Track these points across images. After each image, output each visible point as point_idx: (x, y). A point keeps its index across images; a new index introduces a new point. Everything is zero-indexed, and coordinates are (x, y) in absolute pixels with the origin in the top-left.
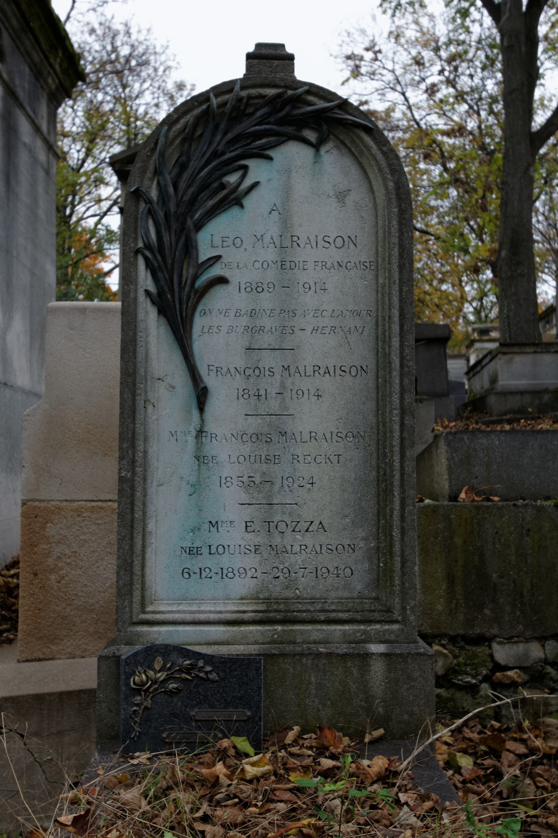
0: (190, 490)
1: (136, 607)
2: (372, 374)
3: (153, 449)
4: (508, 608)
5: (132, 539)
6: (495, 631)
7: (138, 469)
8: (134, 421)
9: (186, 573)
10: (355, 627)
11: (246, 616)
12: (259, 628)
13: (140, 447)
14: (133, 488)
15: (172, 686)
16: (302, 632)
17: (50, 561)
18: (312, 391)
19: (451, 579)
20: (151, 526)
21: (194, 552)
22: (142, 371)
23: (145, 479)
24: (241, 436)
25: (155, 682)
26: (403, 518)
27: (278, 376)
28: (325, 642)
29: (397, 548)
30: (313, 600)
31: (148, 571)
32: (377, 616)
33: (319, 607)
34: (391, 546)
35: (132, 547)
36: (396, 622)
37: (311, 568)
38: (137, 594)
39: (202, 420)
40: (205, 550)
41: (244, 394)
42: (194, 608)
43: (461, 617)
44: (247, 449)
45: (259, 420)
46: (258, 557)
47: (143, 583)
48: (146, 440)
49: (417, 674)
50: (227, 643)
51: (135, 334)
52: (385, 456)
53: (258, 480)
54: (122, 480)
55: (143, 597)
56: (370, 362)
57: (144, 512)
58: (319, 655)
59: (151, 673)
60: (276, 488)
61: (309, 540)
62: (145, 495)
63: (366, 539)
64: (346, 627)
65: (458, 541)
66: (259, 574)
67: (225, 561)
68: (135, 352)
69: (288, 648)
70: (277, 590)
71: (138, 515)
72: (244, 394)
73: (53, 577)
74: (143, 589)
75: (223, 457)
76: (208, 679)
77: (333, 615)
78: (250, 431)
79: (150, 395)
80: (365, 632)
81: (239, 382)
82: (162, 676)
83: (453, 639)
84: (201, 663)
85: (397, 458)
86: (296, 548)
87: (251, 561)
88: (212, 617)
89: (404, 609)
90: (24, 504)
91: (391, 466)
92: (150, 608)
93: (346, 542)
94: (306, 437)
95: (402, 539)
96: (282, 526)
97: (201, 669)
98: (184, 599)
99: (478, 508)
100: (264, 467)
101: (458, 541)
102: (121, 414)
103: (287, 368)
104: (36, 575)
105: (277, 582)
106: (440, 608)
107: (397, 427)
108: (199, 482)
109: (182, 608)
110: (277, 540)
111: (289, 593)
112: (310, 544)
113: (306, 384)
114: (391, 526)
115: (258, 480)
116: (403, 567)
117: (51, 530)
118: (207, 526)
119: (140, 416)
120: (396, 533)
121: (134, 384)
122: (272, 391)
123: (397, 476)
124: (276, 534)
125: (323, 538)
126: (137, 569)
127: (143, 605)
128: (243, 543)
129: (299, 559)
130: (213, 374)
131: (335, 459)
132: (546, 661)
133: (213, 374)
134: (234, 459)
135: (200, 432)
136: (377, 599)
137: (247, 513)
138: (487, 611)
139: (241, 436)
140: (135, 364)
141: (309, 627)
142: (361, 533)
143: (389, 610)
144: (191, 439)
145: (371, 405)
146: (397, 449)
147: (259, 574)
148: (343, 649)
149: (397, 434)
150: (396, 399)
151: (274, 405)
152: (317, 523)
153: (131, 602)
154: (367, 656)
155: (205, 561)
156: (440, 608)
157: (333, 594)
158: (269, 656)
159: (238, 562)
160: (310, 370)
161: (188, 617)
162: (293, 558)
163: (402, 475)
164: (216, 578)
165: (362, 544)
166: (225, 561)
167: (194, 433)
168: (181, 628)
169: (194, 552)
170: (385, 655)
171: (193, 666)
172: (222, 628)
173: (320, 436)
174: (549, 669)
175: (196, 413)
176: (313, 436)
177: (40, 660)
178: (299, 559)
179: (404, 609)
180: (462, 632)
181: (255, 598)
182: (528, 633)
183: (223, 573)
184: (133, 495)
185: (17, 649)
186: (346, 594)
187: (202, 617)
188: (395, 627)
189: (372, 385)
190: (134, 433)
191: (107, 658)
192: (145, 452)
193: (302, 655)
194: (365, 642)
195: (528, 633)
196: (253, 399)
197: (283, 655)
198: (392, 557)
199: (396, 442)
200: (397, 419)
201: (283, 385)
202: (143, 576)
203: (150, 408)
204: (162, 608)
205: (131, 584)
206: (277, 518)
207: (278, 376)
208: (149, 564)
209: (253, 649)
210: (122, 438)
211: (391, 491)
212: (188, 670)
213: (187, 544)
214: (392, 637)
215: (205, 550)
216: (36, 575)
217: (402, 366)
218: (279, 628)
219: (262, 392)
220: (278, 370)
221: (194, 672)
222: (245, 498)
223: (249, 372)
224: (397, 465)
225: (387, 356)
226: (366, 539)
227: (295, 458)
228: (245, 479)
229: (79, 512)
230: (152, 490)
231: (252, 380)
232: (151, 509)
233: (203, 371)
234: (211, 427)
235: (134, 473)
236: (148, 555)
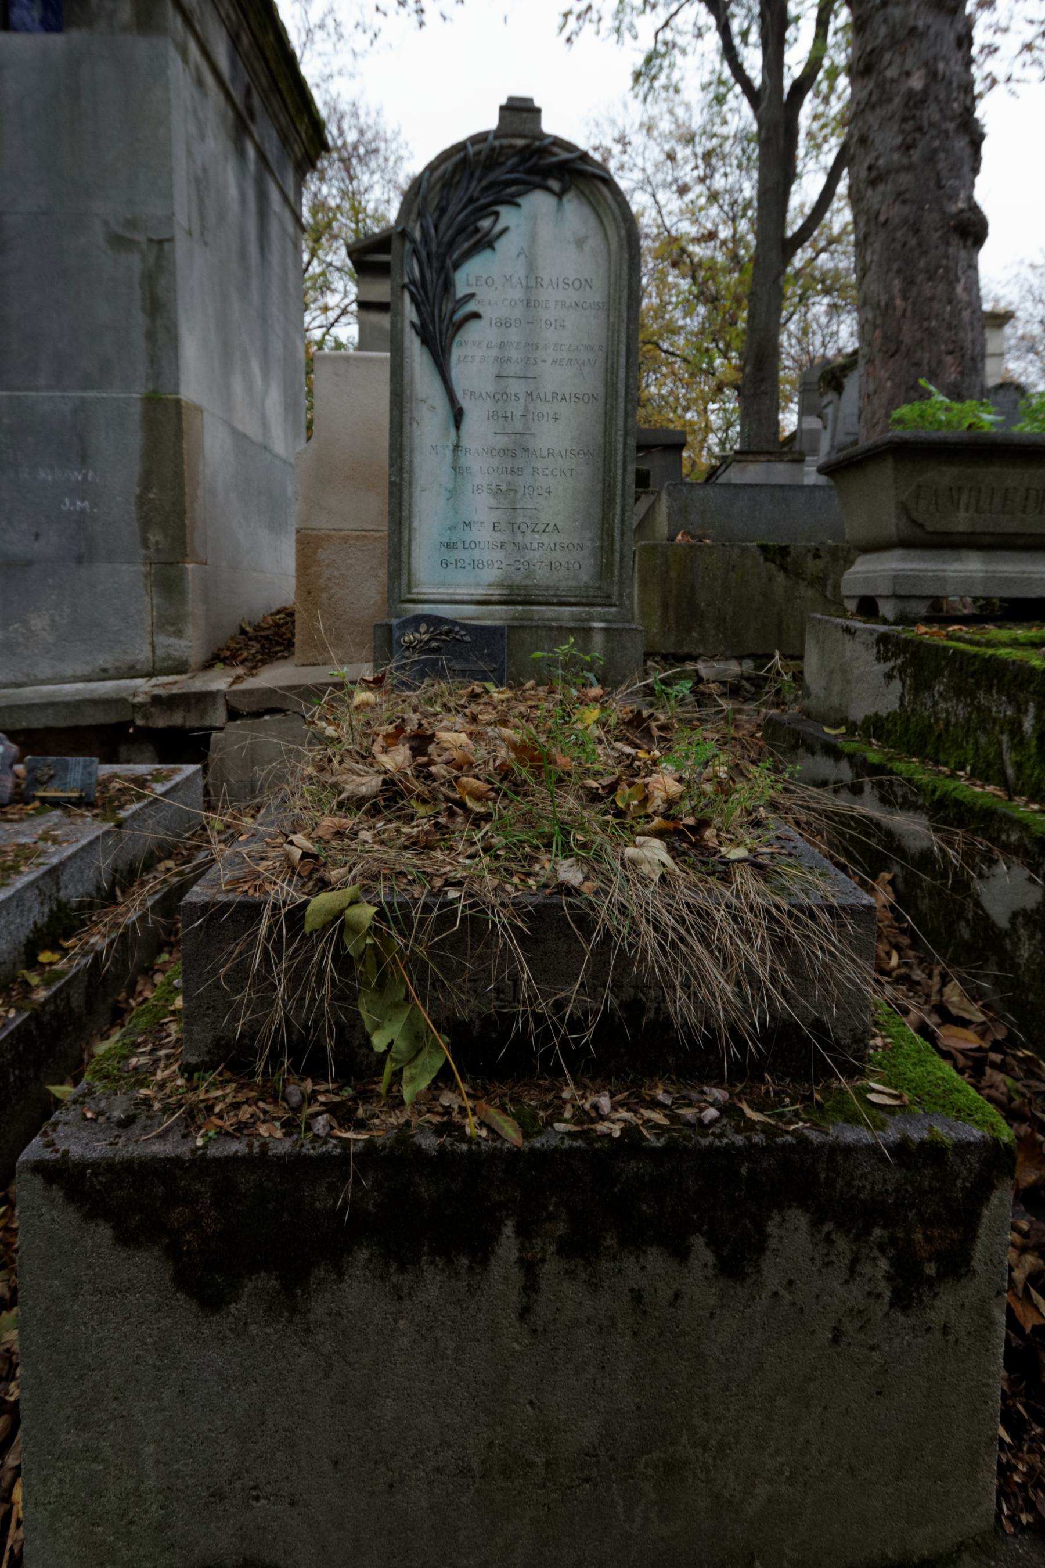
0: (448, 495)
1: (404, 588)
2: (601, 401)
3: (418, 460)
4: (713, 632)
5: (400, 533)
6: (701, 650)
7: (405, 476)
8: (401, 433)
9: (444, 563)
10: (581, 609)
11: (493, 598)
12: (504, 607)
13: (407, 458)
14: (401, 491)
15: (434, 644)
16: (538, 612)
17: (322, 582)
18: (551, 414)
19: (665, 607)
20: (415, 524)
21: (450, 546)
22: (408, 392)
23: (410, 484)
24: (491, 451)
25: (420, 641)
26: (623, 522)
27: (522, 401)
28: (556, 620)
29: (617, 545)
30: (547, 588)
31: (413, 560)
32: (599, 601)
33: (552, 593)
34: (612, 544)
35: (400, 540)
36: (614, 605)
37: (546, 562)
38: (405, 578)
39: (458, 437)
40: (460, 545)
41: (494, 415)
42: (451, 591)
43: (672, 638)
44: (495, 462)
45: (506, 438)
46: (503, 552)
47: (409, 570)
48: (411, 451)
49: (629, 645)
50: (478, 619)
51: (402, 359)
52: (610, 470)
53: (504, 488)
54: (392, 484)
55: (409, 581)
56: (600, 391)
57: (410, 512)
58: (551, 628)
59: (417, 635)
60: (519, 495)
61: (545, 539)
62: (411, 498)
63: (592, 539)
64: (574, 609)
65: (673, 574)
66: (504, 566)
67: (476, 554)
68: (402, 376)
69: (526, 623)
70: (518, 578)
71: (405, 513)
72: (494, 415)
73: (324, 595)
74: (409, 574)
75: (475, 468)
76: (462, 641)
77: (564, 599)
78: (498, 447)
79: (415, 414)
80: (589, 613)
81: (489, 405)
82: (426, 637)
83: (665, 657)
84: (457, 629)
85: (620, 472)
86: (535, 545)
87: (498, 555)
88: (466, 598)
89: (621, 595)
90: (298, 532)
91: (615, 478)
92: (415, 590)
93: (576, 541)
94: (545, 453)
95: (622, 540)
96: (523, 527)
97: (457, 633)
98: (443, 584)
99: (692, 547)
100: (510, 477)
101: (673, 574)
102: (391, 428)
103: (530, 394)
104: (309, 593)
105: (518, 573)
106: (655, 630)
107: (620, 446)
108: (455, 489)
109: (441, 590)
110: (519, 538)
111: (528, 582)
112: (546, 542)
113: (545, 408)
114: (613, 529)
115: (504, 488)
116: (621, 561)
117: (322, 555)
118: (461, 525)
119: (406, 431)
120: (617, 534)
121: (401, 403)
122: (518, 414)
123: (619, 486)
124: (519, 533)
125: (557, 538)
126: (404, 558)
127: (409, 587)
128: (491, 540)
129: (537, 555)
130: (467, 397)
131: (568, 473)
132: (742, 677)
133: (467, 397)
134: (484, 470)
135: (457, 447)
136: (599, 588)
137: (494, 516)
138: (695, 634)
139: (491, 451)
140: (402, 386)
141: (544, 608)
142: (589, 534)
143: (609, 597)
144: (449, 453)
145: (599, 428)
146: (620, 464)
147: (504, 566)
148: (572, 624)
149: (620, 452)
150: (620, 422)
151: (518, 425)
152: (552, 525)
153: (400, 585)
154: (590, 629)
155: (460, 554)
156: (655, 630)
157: (564, 583)
158: (511, 628)
159: (487, 556)
160: (549, 397)
161: (446, 598)
162: (532, 554)
163: (623, 485)
164: (468, 568)
165: (589, 544)
166: (476, 554)
167: (451, 448)
168: (440, 606)
169: (450, 546)
170: (605, 630)
171: (451, 631)
172: (473, 607)
173: (556, 452)
174: (744, 682)
175: (453, 431)
176: (551, 453)
177: (314, 665)
178: (537, 555)
179: (621, 595)
180: (672, 651)
181: (500, 585)
182: (728, 653)
183: (474, 564)
184: (401, 497)
185: (295, 659)
186: (574, 584)
187: (458, 598)
188: (614, 609)
189: (601, 410)
190: (401, 445)
191: (381, 626)
192: (411, 462)
193: (538, 627)
194: (589, 620)
195: (728, 653)
196: (501, 420)
197: (522, 627)
198: (612, 554)
199: (619, 458)
200: (620, 439)
201: (526, 409)
202: (409, 564)
203: (415, 425)
204: (425, 590)
205: (400, 570)
206: (520, 520)
207: (522, 401)
208: (414, 554)
209: (498, 623)
210: (392, 448)
211: (614, 500)
212: (447, 634)
213: (445, 540)
214: (611, 617)
215: (460, 545)
216: (309, 593)
217: (627, 394)
218: (520, 608)
219: (509, 414)
220: (522, 396)
221: (452, 635)
222: (493, 503)
223: (498, 396)
224: (619, 477)
225: (614, 385)
226: (592, 539)
227: (535, 471)
228: (494, 487)
229: (345, 540)
230: (416, 494)
231: (500, 403)
232: (416, 510)
233: (459, 394)
234: (465, 443)
235: (402, 479)
236: (413, 547)
